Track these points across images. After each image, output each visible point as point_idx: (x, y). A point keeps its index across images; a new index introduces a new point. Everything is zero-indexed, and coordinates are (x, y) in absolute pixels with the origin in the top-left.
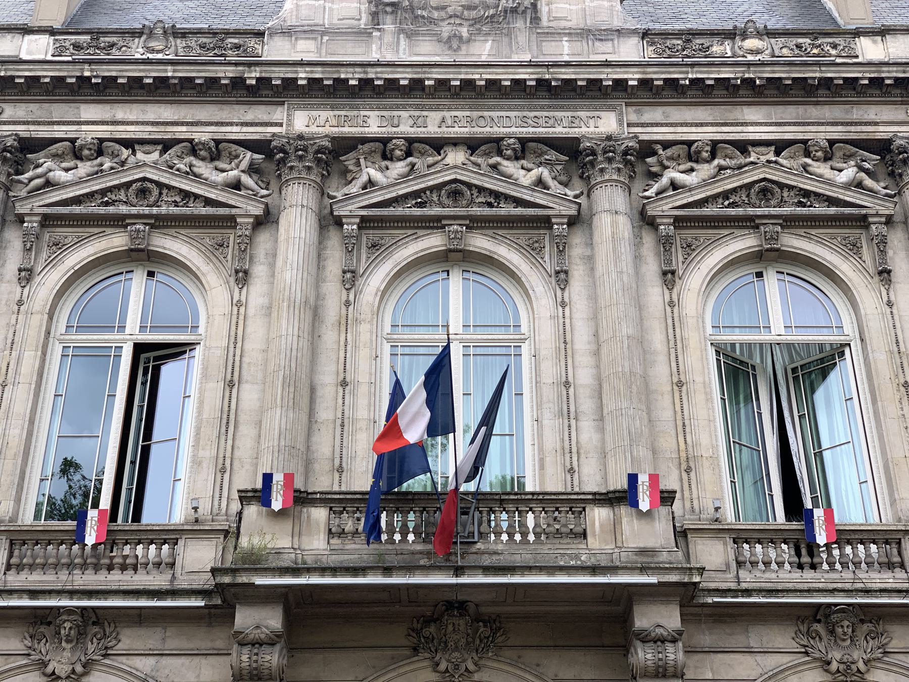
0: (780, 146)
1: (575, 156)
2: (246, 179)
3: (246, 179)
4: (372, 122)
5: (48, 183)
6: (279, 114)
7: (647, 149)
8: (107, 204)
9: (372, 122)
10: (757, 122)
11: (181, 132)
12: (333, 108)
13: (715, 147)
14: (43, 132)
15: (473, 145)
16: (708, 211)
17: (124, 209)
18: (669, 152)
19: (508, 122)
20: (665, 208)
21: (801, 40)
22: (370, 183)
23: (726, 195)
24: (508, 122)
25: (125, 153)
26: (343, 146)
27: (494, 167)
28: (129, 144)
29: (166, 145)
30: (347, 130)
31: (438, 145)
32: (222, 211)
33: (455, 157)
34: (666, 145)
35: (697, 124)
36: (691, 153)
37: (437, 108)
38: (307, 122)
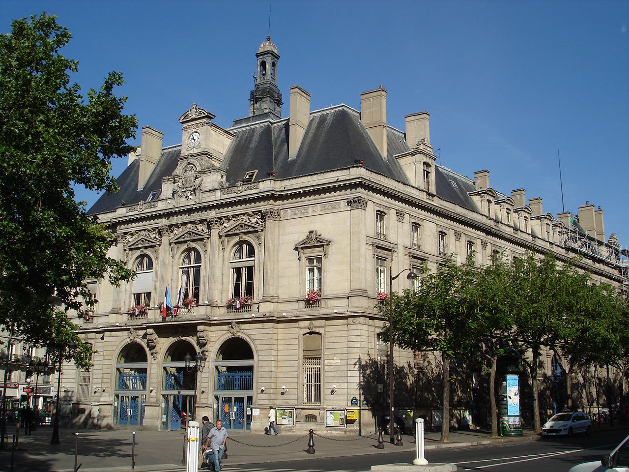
0: (244, 214)
5: (129, 242)
6: (160, 220)
7: (220, 218)
8: (137, 245)
9: (175, 220)
10: (239, 209)
11: (146, 227)
13: (233, 216)
14: (127, 231)
15: (193, 222)
16: (230, 233)
17: (140, 246)
25: (139, 232)
26: (170, 226)
28: (140, 231)
29: (145, 230)
32: (153, 244)
33: (189, 226)
34: (224, 217)
35: (228, 212)
38: (164, 222)
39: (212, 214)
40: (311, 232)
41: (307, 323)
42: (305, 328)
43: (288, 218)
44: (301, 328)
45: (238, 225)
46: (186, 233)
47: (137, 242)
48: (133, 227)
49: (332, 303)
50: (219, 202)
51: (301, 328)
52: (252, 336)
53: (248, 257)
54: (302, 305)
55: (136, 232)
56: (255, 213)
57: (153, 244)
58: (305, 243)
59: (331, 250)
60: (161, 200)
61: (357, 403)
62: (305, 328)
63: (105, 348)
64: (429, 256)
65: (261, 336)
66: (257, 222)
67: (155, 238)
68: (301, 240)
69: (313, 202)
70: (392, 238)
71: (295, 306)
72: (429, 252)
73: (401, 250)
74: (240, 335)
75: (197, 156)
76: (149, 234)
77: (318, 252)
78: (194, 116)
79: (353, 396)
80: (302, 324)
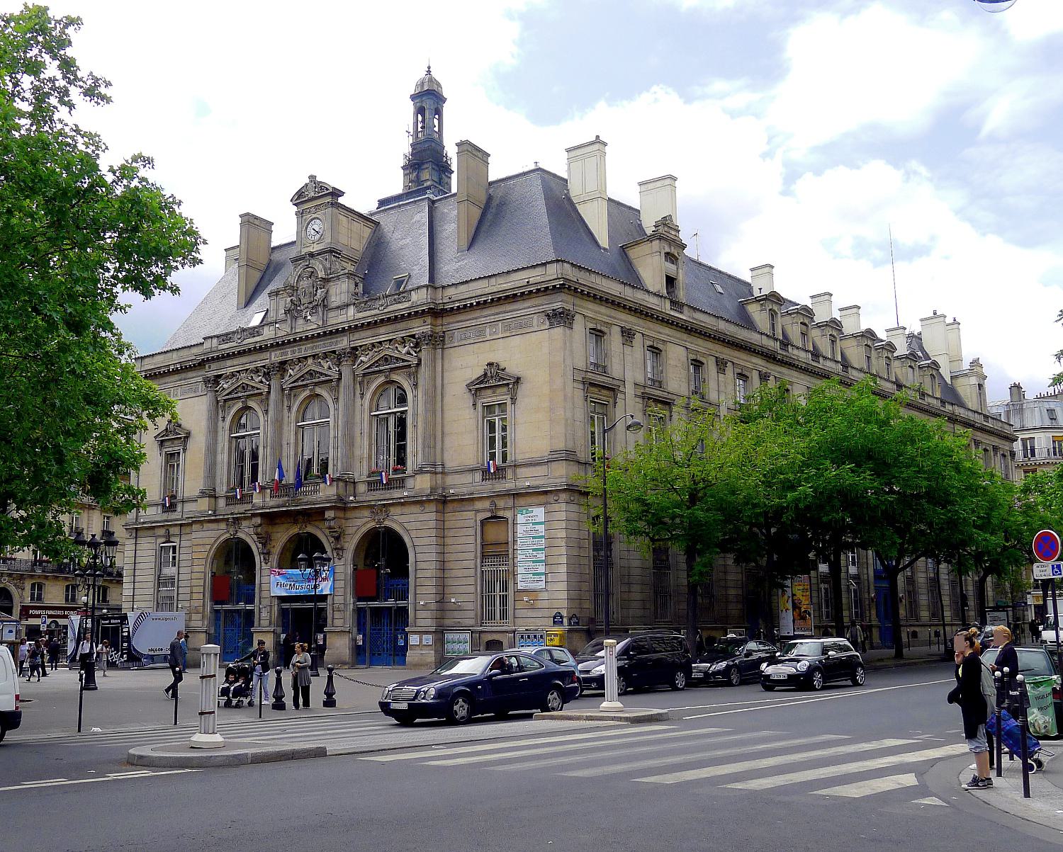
1: (337, 357)
2: (264, 380)
3: (264, 380)
4: (289, 354)
5: (224, 389)
9: (289, 354)
10: (383, 334)
12: (280, 350)
13: (373, 345)
17: (240, 394)
18: (362, 349)
19: (322, 347)
20: (359, 372)
21: (395, 297)
22: (291, 375)
23: (376, 362)
24: (322, 347)
26: (283, 363)
27: (320, 362)
28: (238, 372)
30: (284, 358)
31: (306, 358)
32: (259, 391)
34: (361, 346)
36: (366, 348)
37: (303, 345)
39: (343, 343)
40: (490, 364)
41: (486, 504)
42: (484, 510)
43: (456, 344)
44: (478, 511)
45: (382, 357)
46: (306, 373)
47: (235, 389)
48: (229, 367)
49: (522, 472)
50: (352, 324)
51: (478, 511)
52: (405, 525)
53: (398, 407)
54: (478, 476)
55: (233, 375)
56: (403, 341)
57: (259, 391)
58: (481, 382)
59: (523, 390)
60: (268, 324)
61: (562, 622)
62: (484, 510)
63: (195, 549)
64: (675, 397)
65: (418, 525)
66: (409, 353)
67: (261, 382)
68: (475, 377)
69: (492, 318)
70: (615, 370)
71: (467, 478)
72: (674, 392)
73: (629, 390)
74: (387, 523)
75: (319, 254)
76: (252, 377)
77: (502, 396)
78: (312, 194)
79: (556, 611)
80: (479, 505)
